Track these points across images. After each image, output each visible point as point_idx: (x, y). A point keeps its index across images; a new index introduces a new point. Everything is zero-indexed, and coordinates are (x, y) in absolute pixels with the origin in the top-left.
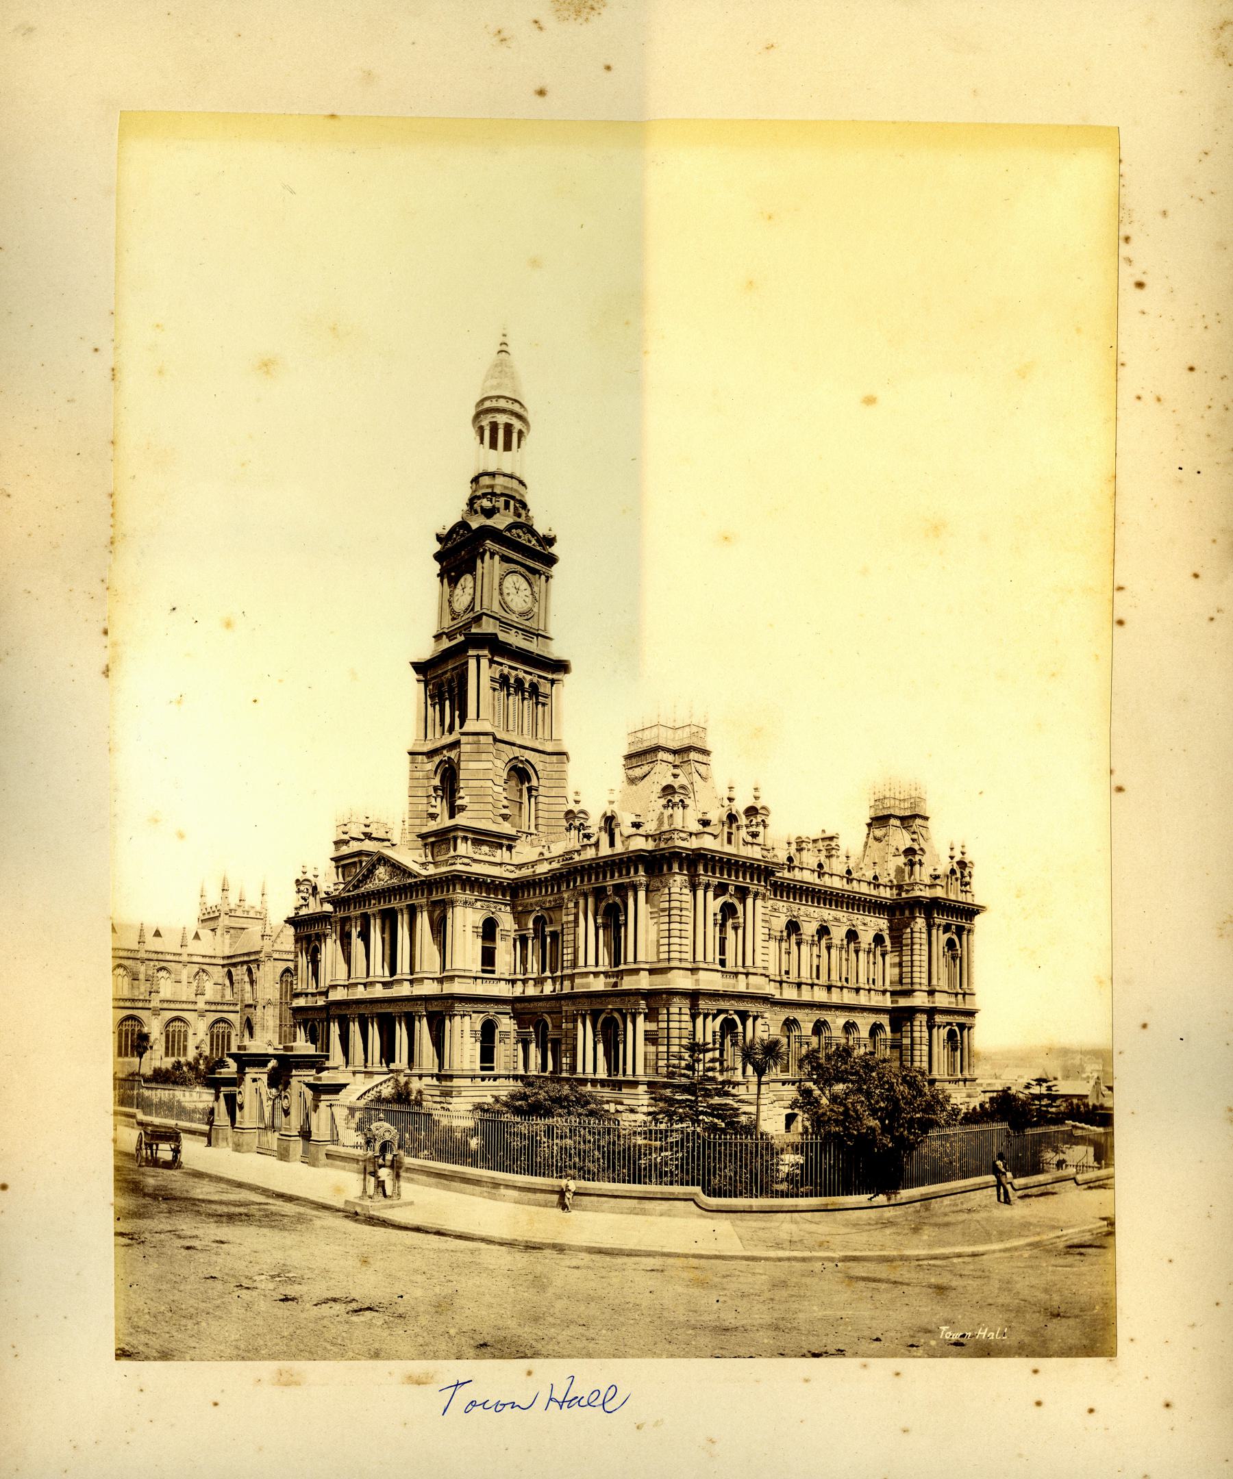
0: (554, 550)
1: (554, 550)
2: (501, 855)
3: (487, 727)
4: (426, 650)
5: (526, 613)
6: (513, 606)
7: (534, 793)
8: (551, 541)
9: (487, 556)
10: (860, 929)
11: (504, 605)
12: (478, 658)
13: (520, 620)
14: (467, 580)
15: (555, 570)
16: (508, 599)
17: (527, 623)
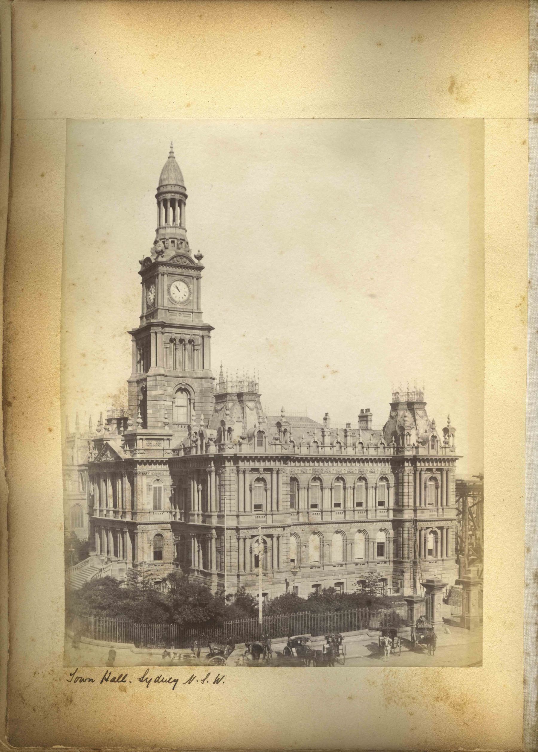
0: (203, 262)
1: (203, 262)
2: (165, 444)
3: (162, 371)
4: (136, 324)
5: (185, 301)
6: (177, 299)
7: (192, 401)
8: (199, 257)
9: (160, 276)
10: (368, 475)
11: (172, 300)
12: (156, 333)
13: (181, 306)
14: (153, 288)
15: (203, 273)
16: (173, 296)
17: (185, 307)
